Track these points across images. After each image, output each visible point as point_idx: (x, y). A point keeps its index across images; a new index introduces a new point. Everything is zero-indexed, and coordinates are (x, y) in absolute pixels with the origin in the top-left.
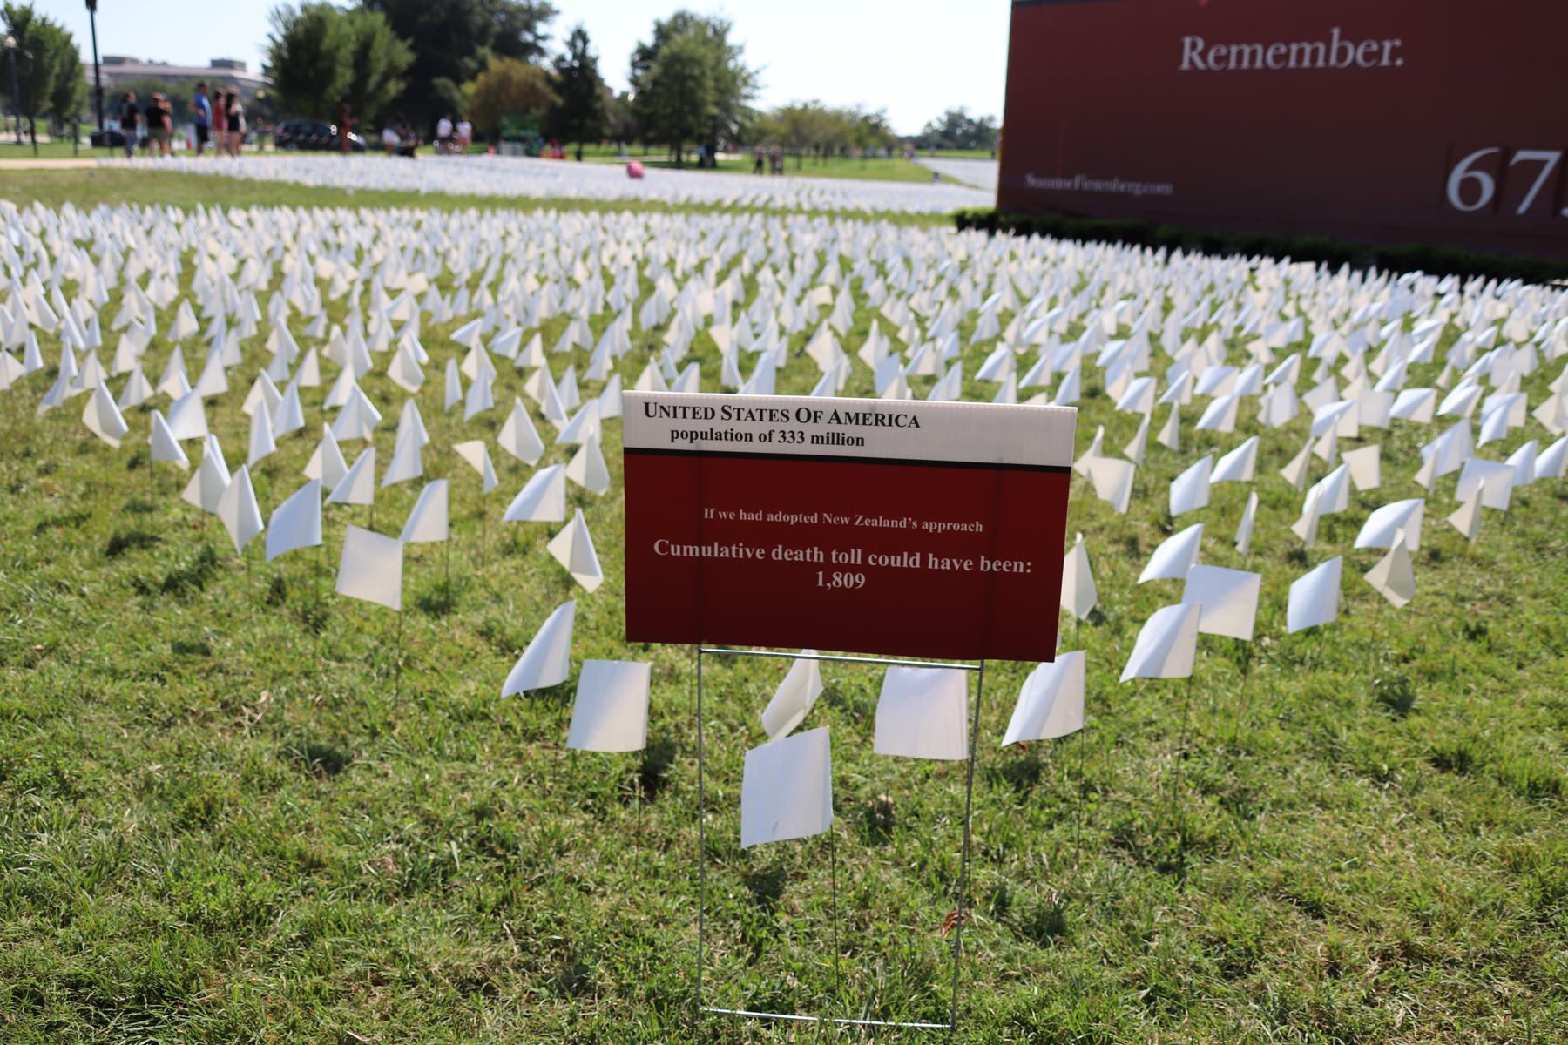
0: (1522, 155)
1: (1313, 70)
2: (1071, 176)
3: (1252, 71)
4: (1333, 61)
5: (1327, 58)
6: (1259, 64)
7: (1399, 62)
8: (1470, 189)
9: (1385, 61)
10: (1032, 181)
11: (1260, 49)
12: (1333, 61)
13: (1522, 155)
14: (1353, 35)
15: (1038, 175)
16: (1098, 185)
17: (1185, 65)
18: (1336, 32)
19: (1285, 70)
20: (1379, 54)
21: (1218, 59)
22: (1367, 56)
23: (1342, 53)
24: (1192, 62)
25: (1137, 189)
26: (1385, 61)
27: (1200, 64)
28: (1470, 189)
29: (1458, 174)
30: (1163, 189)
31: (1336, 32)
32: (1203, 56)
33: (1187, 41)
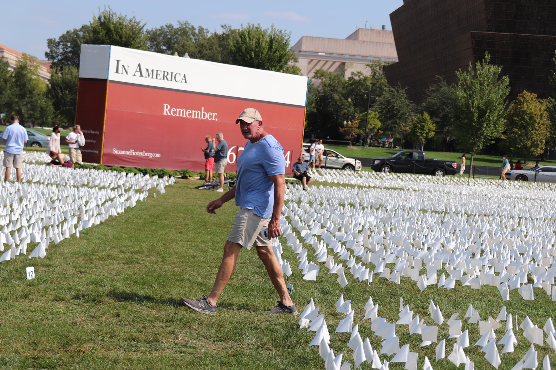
1: (198, 120)
2: (129, 150)
3: (182, 117)
5: (201, 117)
8: (231, 156)
10: (116, 152)
14: (207, 110)
15: (117, 150)
16: (138, 154)
17: (165, 114)
18: (203, 108)
19: (191, 119)
21: (174, 113)
22: (210, 117)
23: (204, 114)
24: (166, 113)
25: (150, 155)
27: (169, 114)
30: (158, 155)
31: (203, 108)
32: (170, 111)
33: (165, 105)
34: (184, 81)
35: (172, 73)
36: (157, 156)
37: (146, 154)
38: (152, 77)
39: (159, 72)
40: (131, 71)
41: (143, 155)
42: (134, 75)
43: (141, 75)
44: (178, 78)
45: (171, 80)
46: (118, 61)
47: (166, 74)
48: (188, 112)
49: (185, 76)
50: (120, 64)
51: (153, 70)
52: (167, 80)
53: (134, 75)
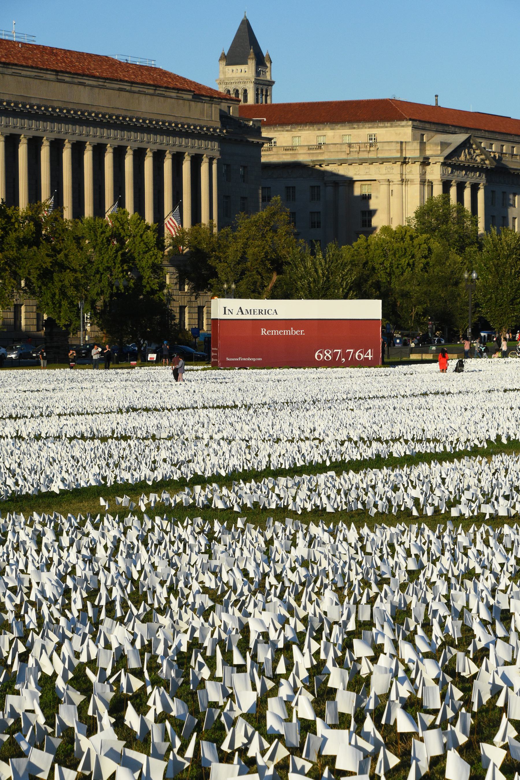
8: (319, 357)
28: (319, 357)
29: (317, 354)
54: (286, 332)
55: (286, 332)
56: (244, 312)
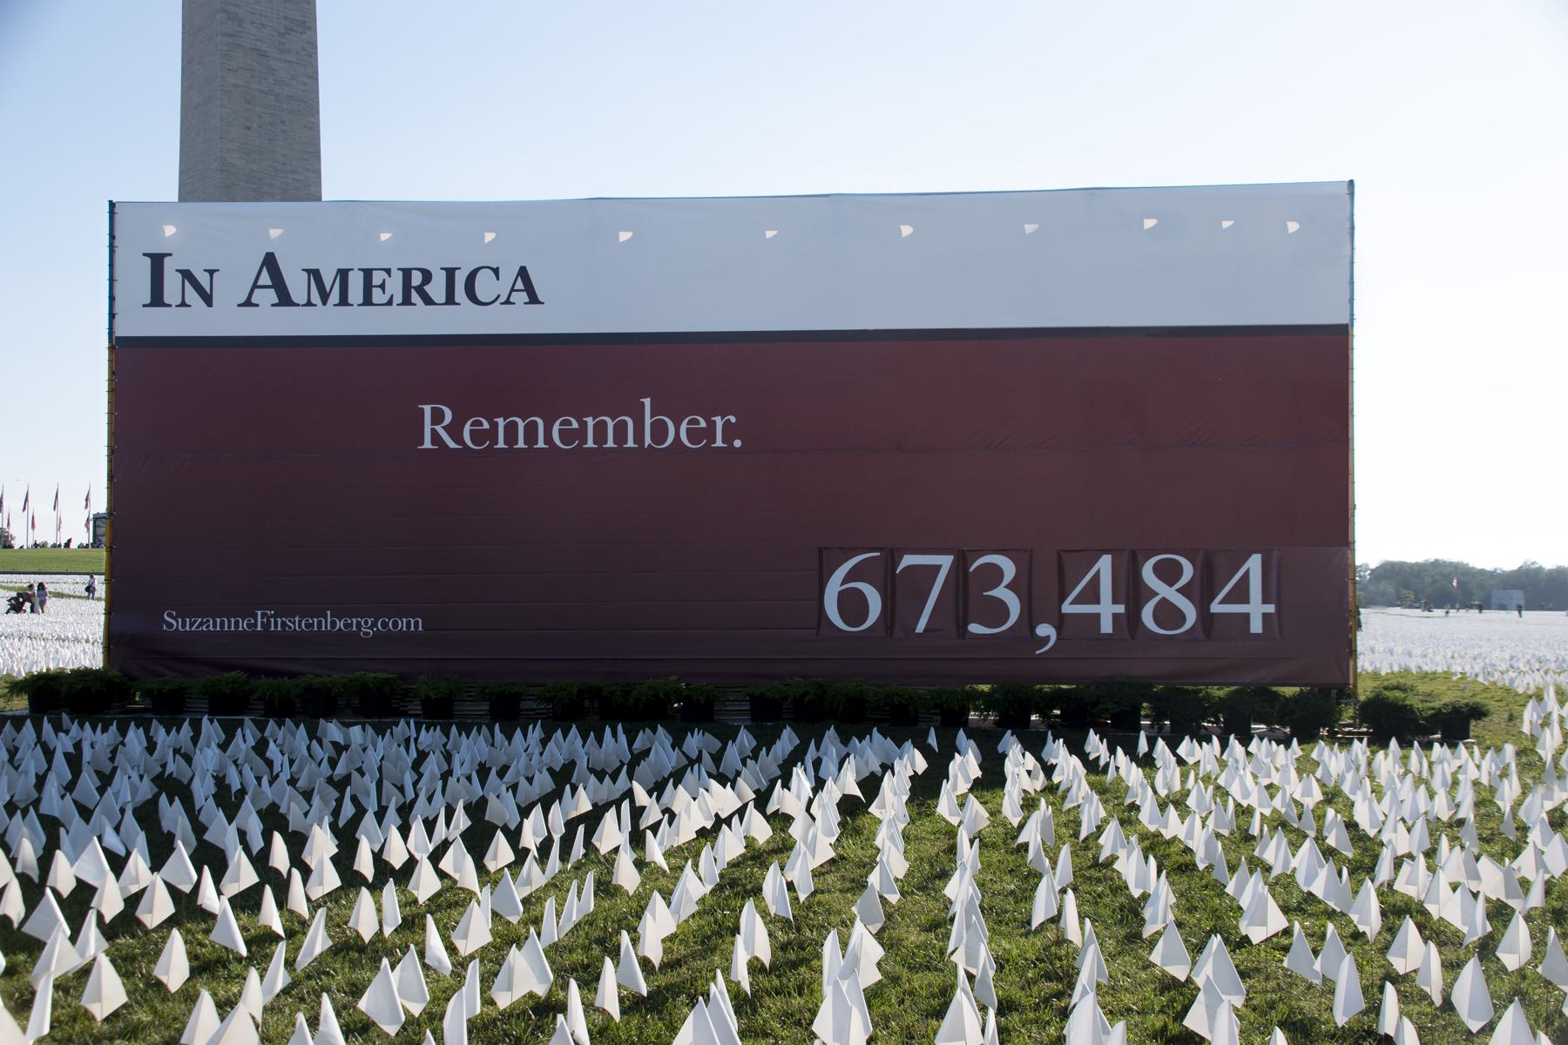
0: (908, 560)
1: (620, 450)
4: (648, 441)
5: (639, 437)
6: (541, 444)
7: (737, 443)
8: (853, 605)
9: (719, 443)
11: (540, 422)
12: (648, 441)
13: (908, 560)
15: (182, 615)
16: (297, 624)
17: (428, 444)
18: (647, 401)
19: (581, 451)
20: (710, 432)
22: (693, 435)
23: (659, 431)
24: (436, 437)
25: (366, 627)
26: (719, 443)
27: (452, 444)
28: (853, 605)
31: (647, 401)
33: (427, 409)
34: (524, 297)
35: (450, 273)
36: (402, 624)
37: (340, 624)
38: (344, 301)
39: (377, 278)
40: (229, 290)
41: (326, 625)
42: (248, 303)
43: (285, 299)
44: (486, 286)
45: (450, 300)
46: (157, 261)
47: (417, 279)
48: (556, 427)
49: (523, 273)
50: (170, 267)
51: (343, 274)
52: (428, 301)
53: (248, 303)
54: (601, 431)
55: (601, 431)
56: (297, 286)
